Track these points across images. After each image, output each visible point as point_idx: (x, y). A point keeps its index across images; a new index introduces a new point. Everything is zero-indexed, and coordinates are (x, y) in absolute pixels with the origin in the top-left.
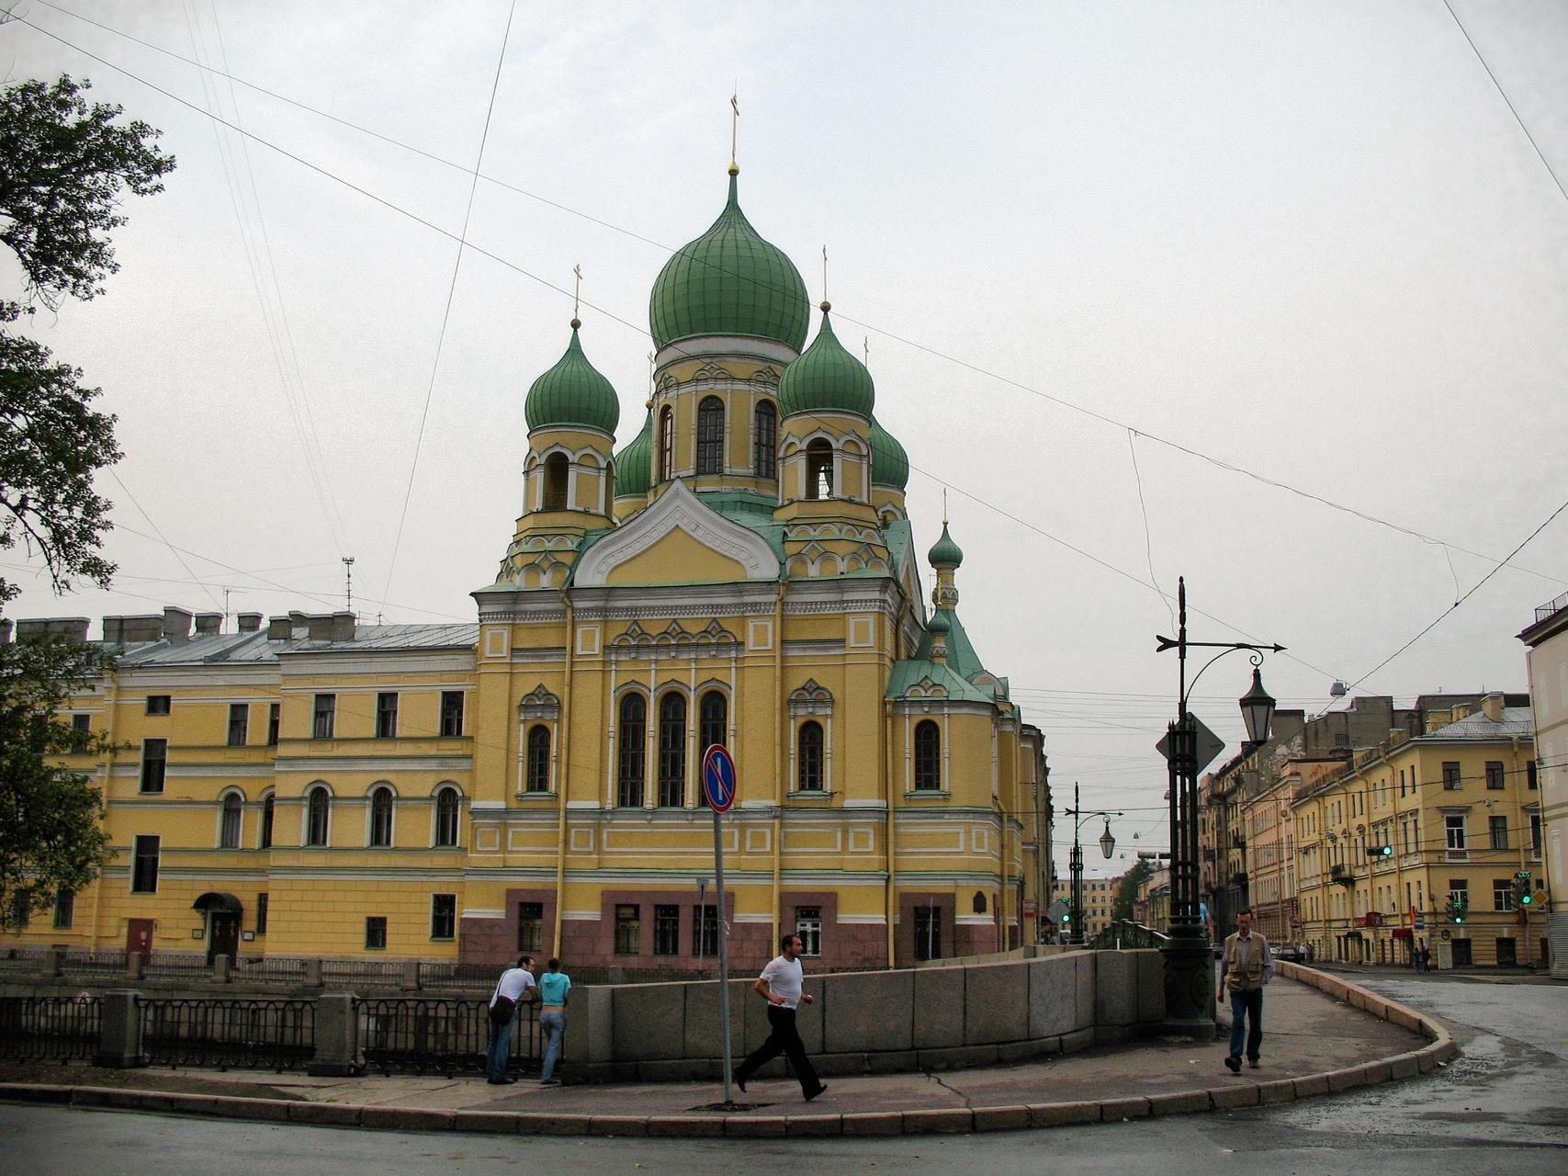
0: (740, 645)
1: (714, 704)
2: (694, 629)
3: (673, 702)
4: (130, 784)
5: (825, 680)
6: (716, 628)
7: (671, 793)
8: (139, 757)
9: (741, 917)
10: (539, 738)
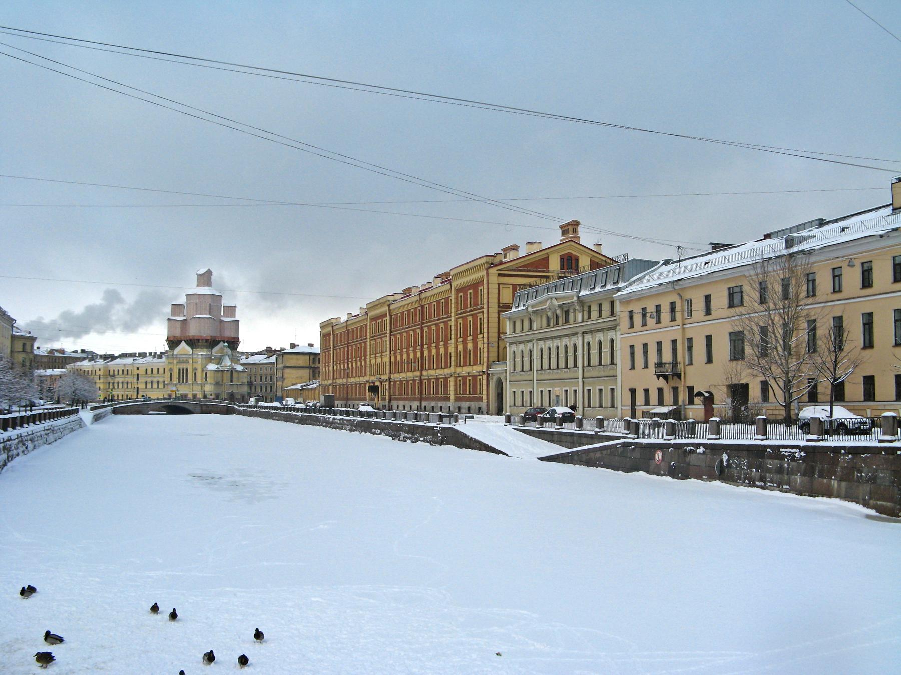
0: (188, 362)
1: (187, 370)
2: (185, 360)
3: (183, 370)
4: (135, 380)
5: (196, 367)
6: (187, 361)
7: (183, 382)
8: (136, 376)
9: (198, 397)
10: (171, 374)
